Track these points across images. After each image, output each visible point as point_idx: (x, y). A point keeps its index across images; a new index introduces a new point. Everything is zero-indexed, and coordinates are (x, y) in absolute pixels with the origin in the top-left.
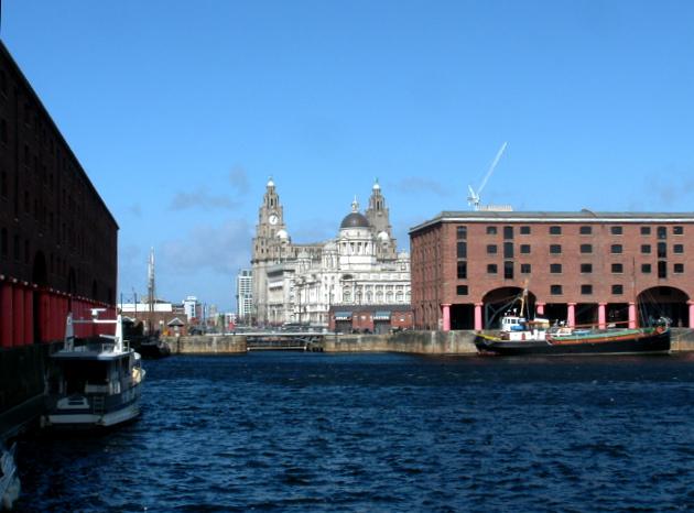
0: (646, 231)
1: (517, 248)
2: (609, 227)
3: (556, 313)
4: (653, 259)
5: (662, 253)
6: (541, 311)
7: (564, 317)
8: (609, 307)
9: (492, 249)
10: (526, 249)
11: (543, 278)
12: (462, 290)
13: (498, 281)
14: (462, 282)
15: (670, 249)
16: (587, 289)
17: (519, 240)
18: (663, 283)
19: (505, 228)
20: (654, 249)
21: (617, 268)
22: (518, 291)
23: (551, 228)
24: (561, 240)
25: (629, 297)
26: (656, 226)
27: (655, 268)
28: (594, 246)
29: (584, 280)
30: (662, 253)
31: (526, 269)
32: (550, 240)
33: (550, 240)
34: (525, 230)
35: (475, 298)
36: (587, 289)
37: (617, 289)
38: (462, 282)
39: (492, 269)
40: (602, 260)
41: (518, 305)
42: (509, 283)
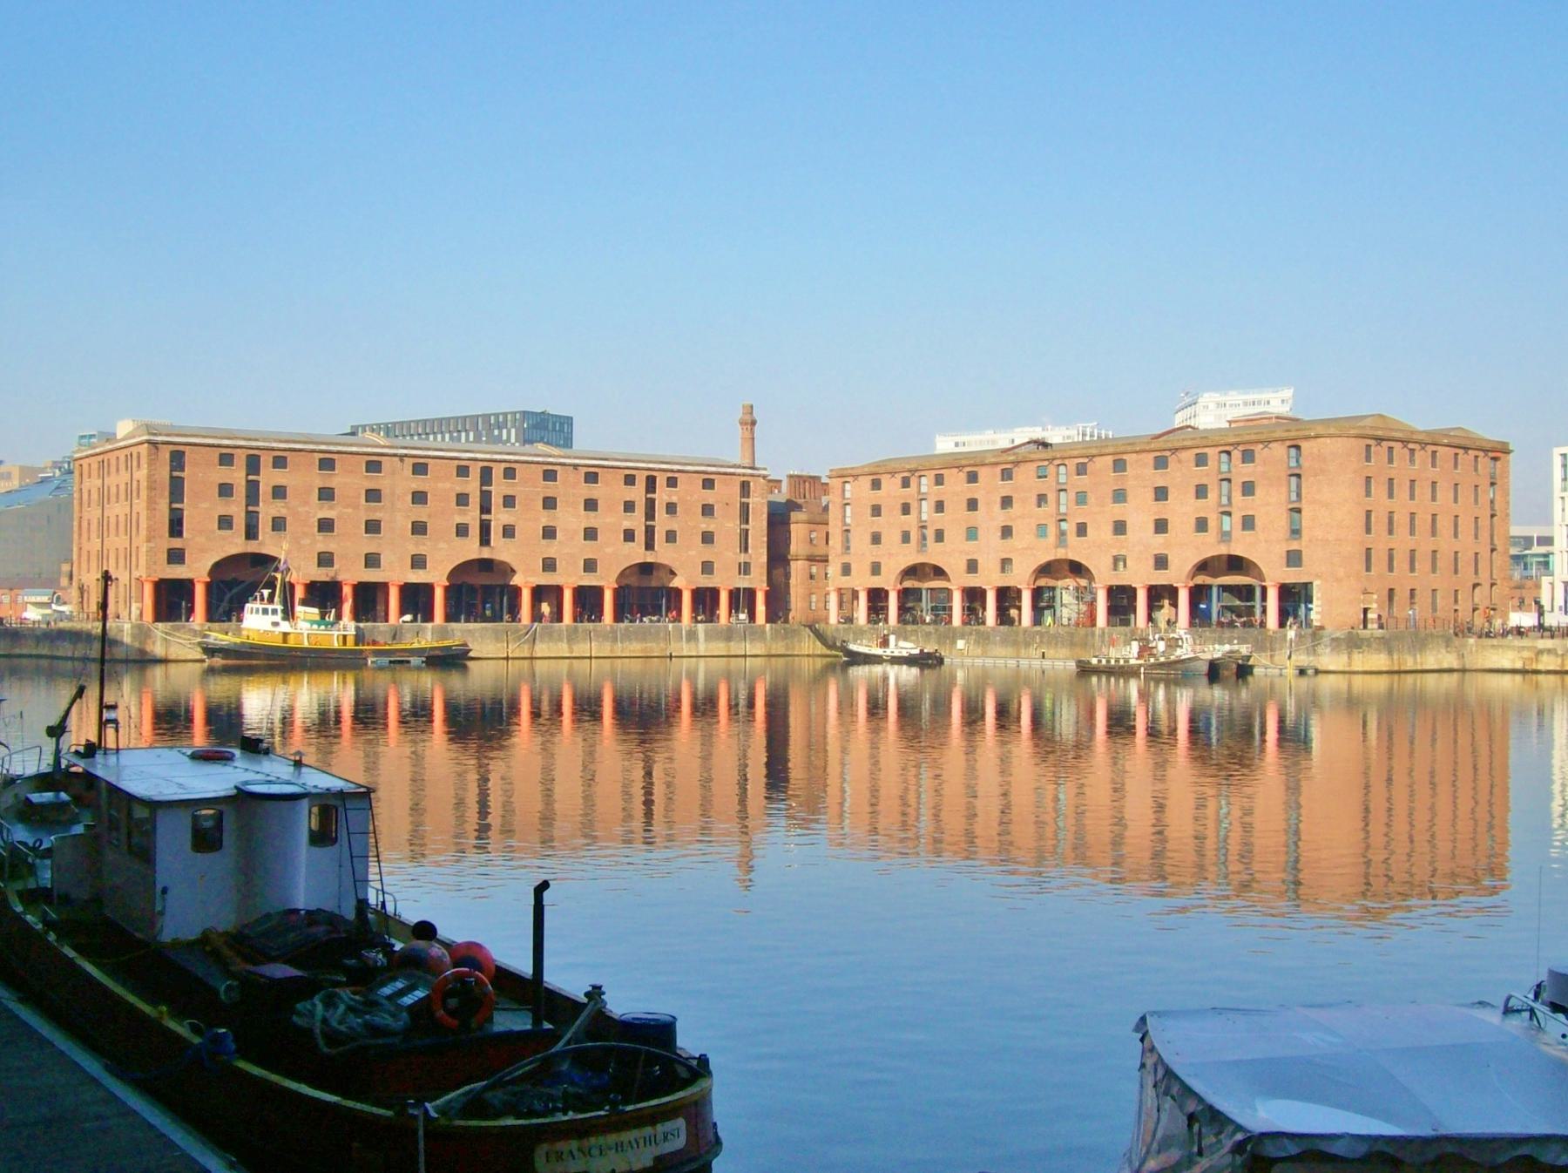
0: (463, 471)
1: (265, 490)
2: (409, 462)
3: (324, 595)
4: (472, 516)
5: (485, 508)
6: (299, 593)
7: (338, 605)
8: (734, 595)
9: (225, 490)
10: (279, 492)
11: (306, 541)
12: (176, 556)
13: (236, 544)
14: (176, 543)
15: (496, 500)
16: (325, 560)
17: (269, 477)
18: (486, 553)
19: (249, 457)
20: (475, 500)
21: (419, 528)
22: (264, 561)
23: (414, 465)
24: (336, 480)
25: (437, 576)
26: (504, 465)
27: (475, 531)
28: (385, 493)
29: (369, 544)
30: (485, 508)
31: (278, 524)
32: (318, 479)
33: (318, 479)
34: (280, 462)
35: (197, 570)
36: (372, 561)
37: (418, 562)
38: (176, 543)
39: (225, 522)
40: (398, 515)
41: (271, 584)
42: (252, 547)
